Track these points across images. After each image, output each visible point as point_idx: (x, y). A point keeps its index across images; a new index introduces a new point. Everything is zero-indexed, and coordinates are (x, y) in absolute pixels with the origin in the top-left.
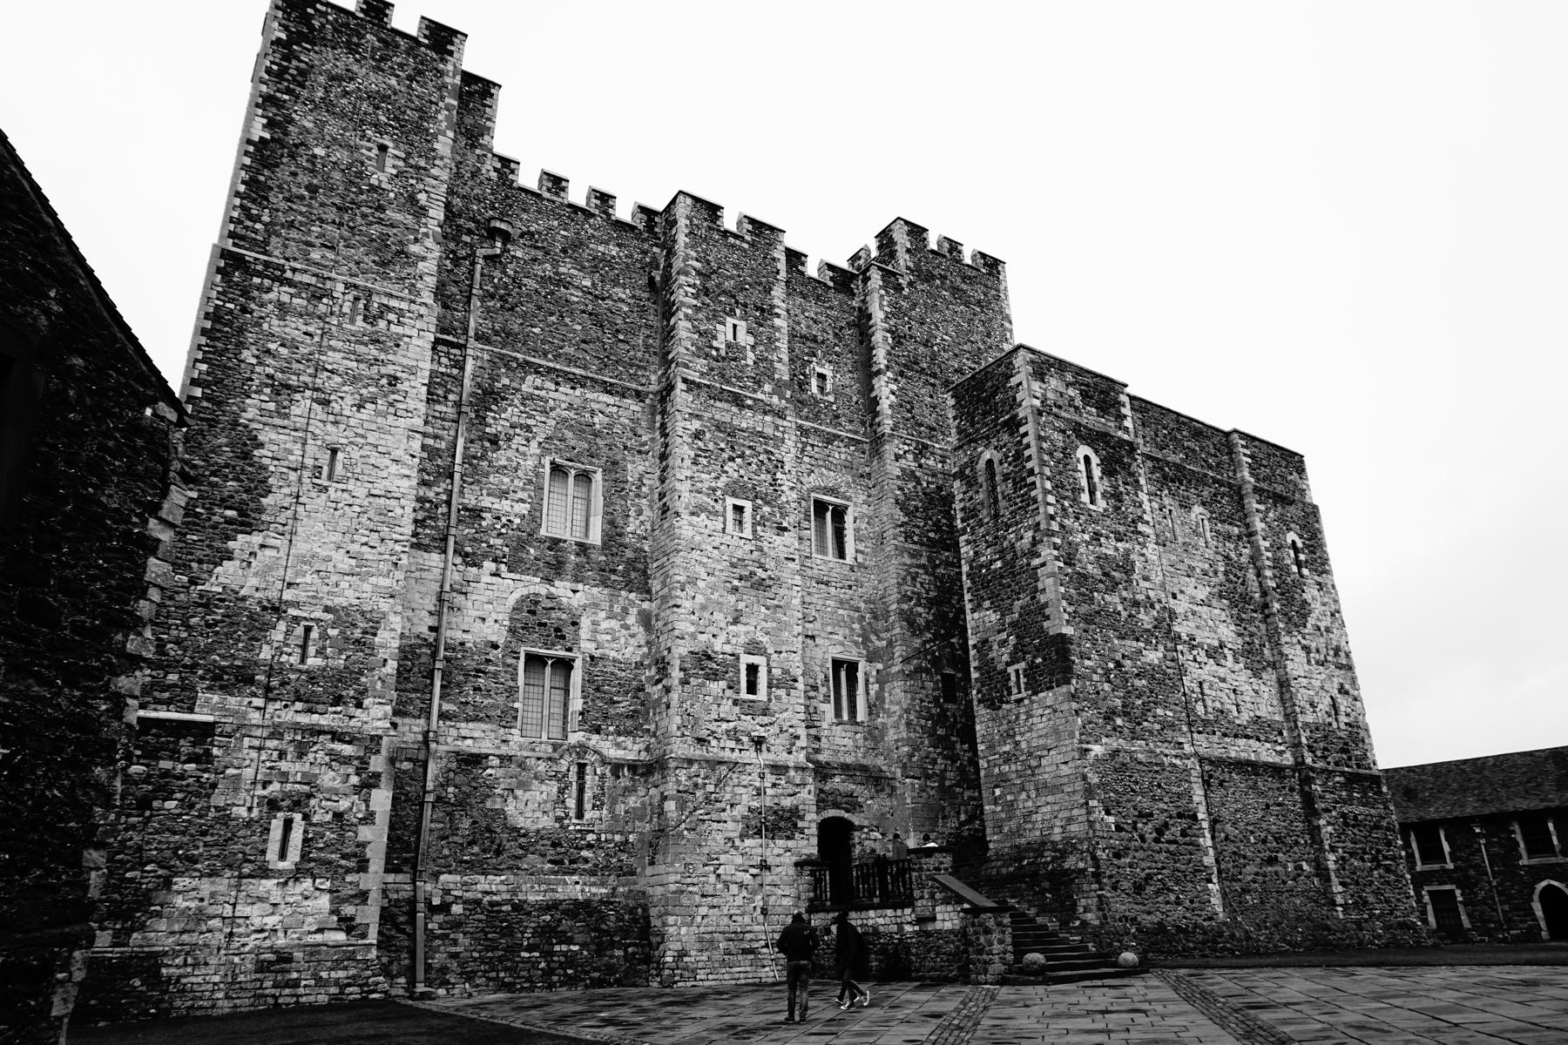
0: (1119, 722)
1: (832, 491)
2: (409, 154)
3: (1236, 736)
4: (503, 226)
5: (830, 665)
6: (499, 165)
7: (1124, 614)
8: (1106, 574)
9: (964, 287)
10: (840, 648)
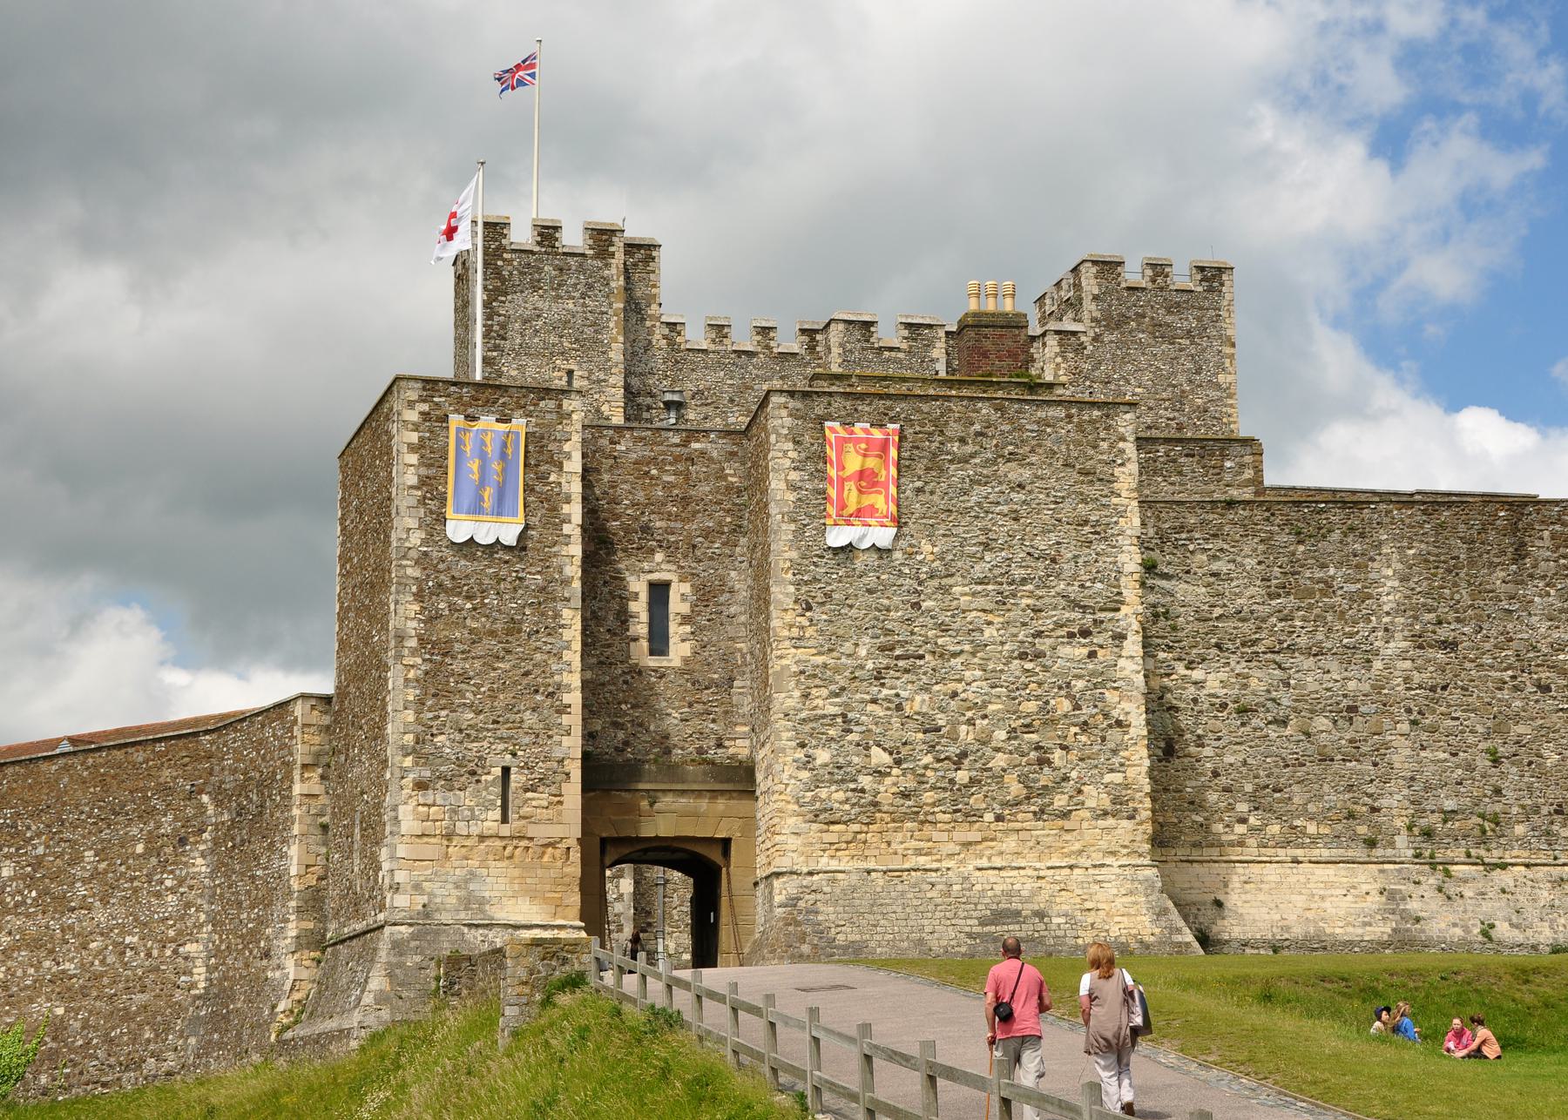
2: (591, 372)
4: (676, 398)
6: (666, 331)
9: (1169, 319)
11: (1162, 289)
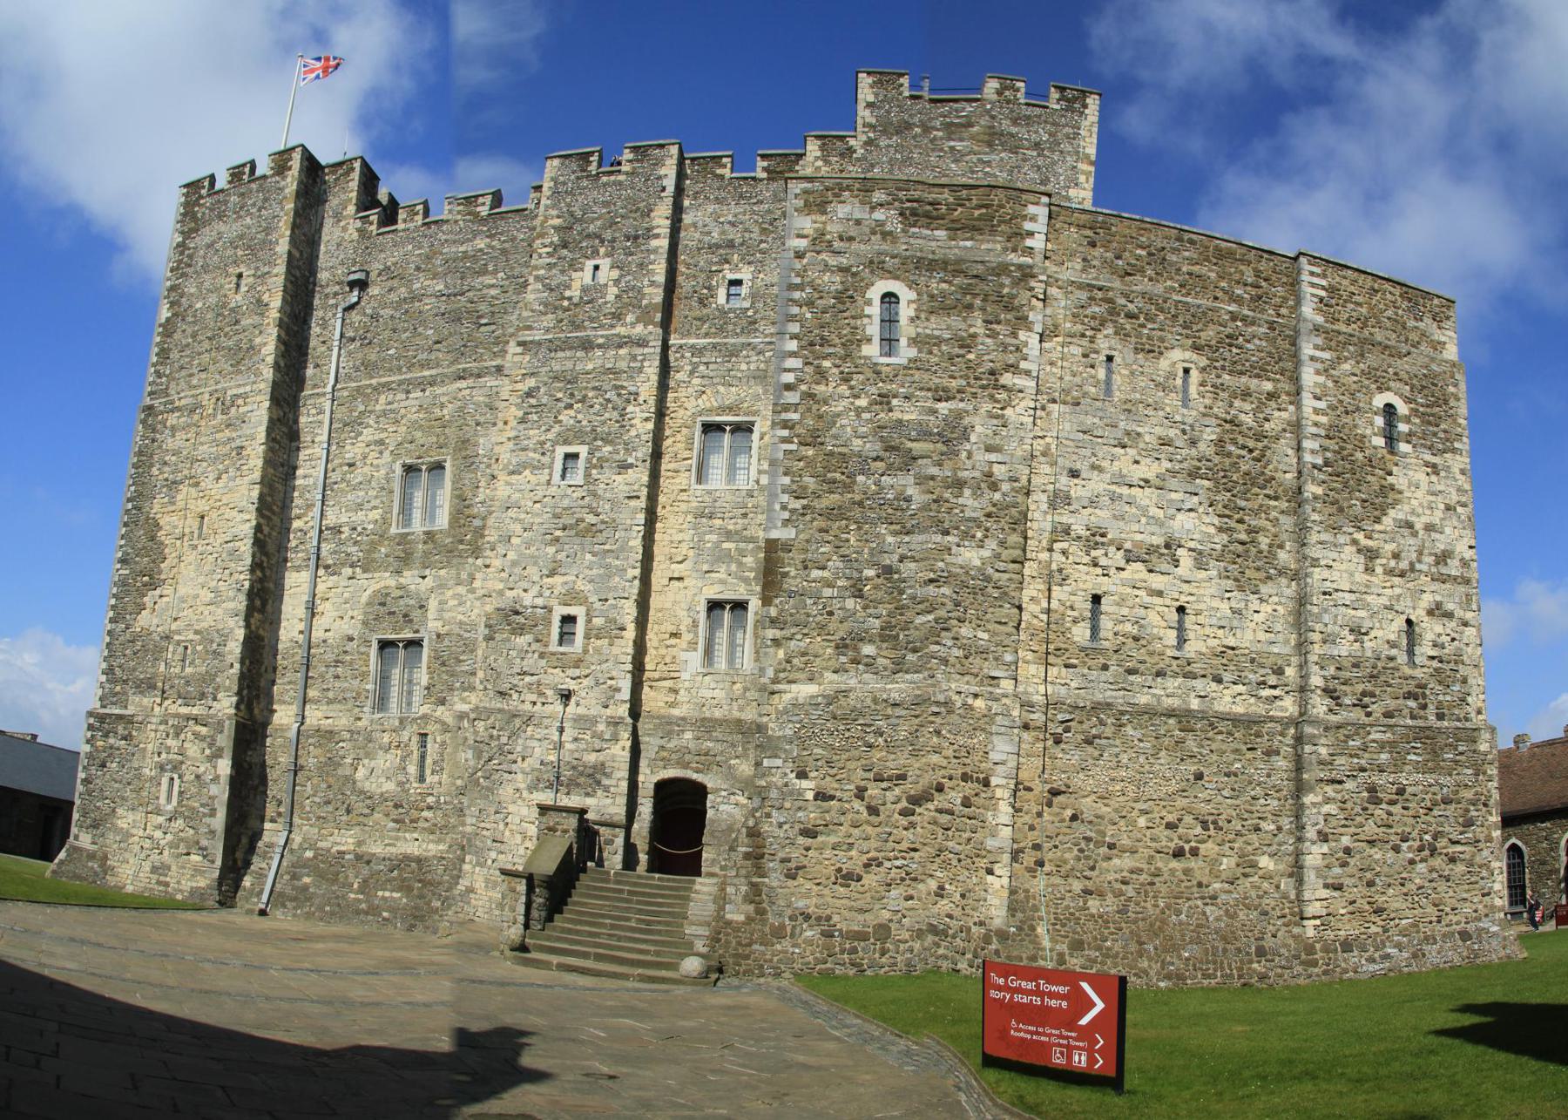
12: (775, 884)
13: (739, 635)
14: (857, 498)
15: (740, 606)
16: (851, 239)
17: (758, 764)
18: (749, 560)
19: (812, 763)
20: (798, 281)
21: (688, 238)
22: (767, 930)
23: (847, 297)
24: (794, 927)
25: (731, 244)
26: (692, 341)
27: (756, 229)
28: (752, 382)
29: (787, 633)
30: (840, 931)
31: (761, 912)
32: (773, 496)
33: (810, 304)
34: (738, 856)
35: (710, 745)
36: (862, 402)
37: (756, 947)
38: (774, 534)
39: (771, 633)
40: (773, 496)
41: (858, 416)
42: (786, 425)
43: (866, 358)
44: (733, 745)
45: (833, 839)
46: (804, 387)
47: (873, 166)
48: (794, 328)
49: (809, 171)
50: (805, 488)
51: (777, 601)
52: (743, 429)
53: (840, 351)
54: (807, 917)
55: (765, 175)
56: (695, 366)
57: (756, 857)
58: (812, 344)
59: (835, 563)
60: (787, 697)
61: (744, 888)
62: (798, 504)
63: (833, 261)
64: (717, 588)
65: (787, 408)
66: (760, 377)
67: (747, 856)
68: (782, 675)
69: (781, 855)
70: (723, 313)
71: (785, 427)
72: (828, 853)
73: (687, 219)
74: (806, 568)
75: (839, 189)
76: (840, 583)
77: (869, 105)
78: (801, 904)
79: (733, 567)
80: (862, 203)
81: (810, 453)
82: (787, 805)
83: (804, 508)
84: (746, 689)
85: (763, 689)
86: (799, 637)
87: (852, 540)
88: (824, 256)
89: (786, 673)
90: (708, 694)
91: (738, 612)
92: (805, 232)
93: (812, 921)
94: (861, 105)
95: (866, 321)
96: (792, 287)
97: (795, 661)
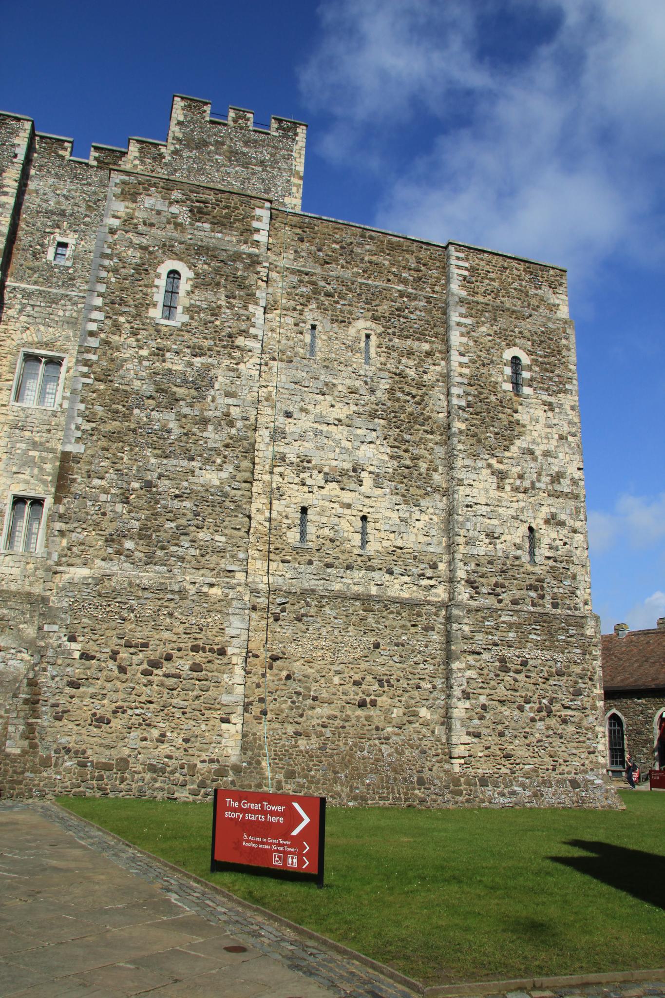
0: (129, 544)
1: (46, 345)
3: (349, 567)
5: (9, 501)
7: (177, 431)
8: (160, 391)
9: (245, 150)
10: (22, 486)
11: (241, 128)
12: (46, 724)
13: (35, 525)
14: (133, 426)
15: (38, 502)
16: (152, 225)
17: (40, 629)
18: (48, 467)
19: (80, 630)
20: (109, 251)
21: (31, 201)
22: (37, 760)
23: (143, 270)
24: (58, 758)
25: (63, 213)
26: (24, 286)
27: (84, 205)
28: (66, 326)
29: (70, 526)
30: (92, 762)
31: (33, 746)
32: (70, 418)
33: (115, 271)
34: (19, 702)
35: (5, 611)
36: (144, 353)
37: (28, 774)
38: (69, 448)
39: (59, 526)
40: (70, 418)
41: (140, 363)
42: (86, 363)
43: (151, 318)
44: (23, 613)
45: (91, 690)
46: (103, 336)
47: (175, 171)
48: (102, 288)
49: (128, 167)
50: (95, 414)
51: (65, 501)
52: (55, 362)
53: (133, 310)
54: (68, 751)
55: (95, 163)
56: (24, 306)
57: (33, 702)
58: (113, 303)
59: (111, 475)
60: (66, 577)
61: (21, 727)
62: (88, 426)
63: (136, 240)
64: (22, 486)
65: (88, 350)
66: (72, 323)
67: (26, 702)
68: (64, 559)
69: (52, 701)
70: (50, 267)
71: (85, 365)
72: (87, 701)
73: (32, 185)
74: (89, 477)
75: (148, 184)
76: (113, 491)
77: (180, 123)
78: (64, 740)
79: (36, 471)
80: (164, 198)
81: (102, 387)
82: (60, 662)
83: (93, 429)
84: (36, 569)
85: (48, 569)
86: (79, 530)
87: (126, 458)
88: (130, 235)
89: (67, 558)
90: (8, 571)
91: (36, 507)
92: (119, 214)
93: (72, 754)
94: (173, 122)
95: (155, 290)
96: (104, 256)
97: (75, 549)
